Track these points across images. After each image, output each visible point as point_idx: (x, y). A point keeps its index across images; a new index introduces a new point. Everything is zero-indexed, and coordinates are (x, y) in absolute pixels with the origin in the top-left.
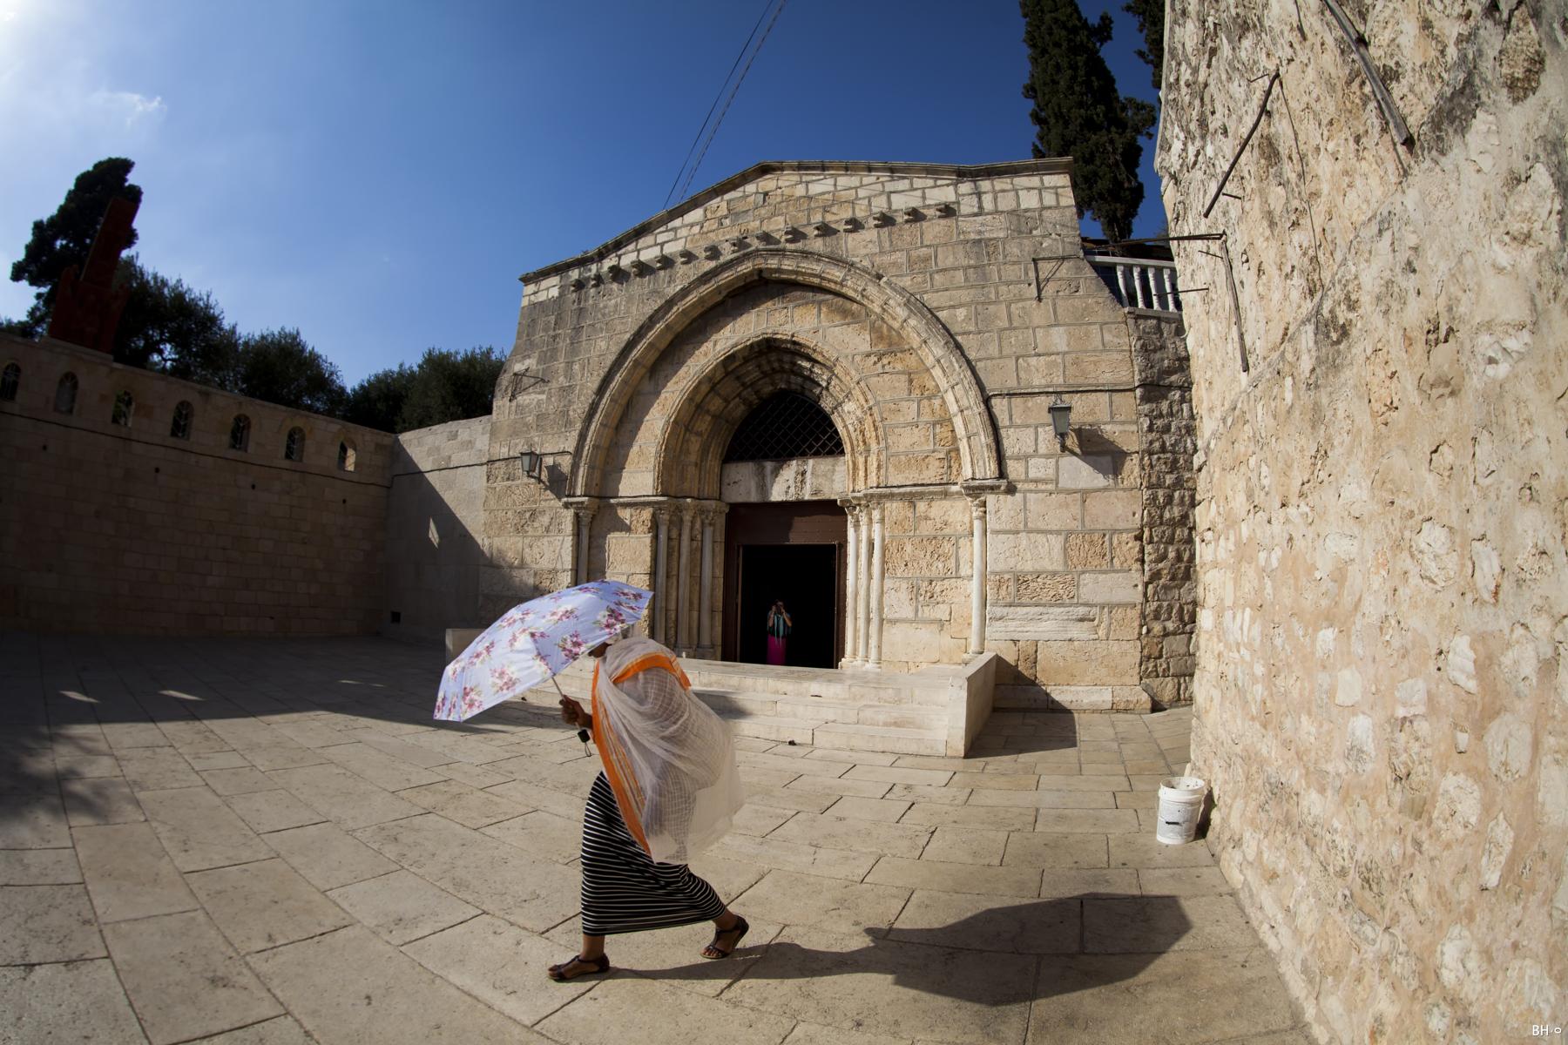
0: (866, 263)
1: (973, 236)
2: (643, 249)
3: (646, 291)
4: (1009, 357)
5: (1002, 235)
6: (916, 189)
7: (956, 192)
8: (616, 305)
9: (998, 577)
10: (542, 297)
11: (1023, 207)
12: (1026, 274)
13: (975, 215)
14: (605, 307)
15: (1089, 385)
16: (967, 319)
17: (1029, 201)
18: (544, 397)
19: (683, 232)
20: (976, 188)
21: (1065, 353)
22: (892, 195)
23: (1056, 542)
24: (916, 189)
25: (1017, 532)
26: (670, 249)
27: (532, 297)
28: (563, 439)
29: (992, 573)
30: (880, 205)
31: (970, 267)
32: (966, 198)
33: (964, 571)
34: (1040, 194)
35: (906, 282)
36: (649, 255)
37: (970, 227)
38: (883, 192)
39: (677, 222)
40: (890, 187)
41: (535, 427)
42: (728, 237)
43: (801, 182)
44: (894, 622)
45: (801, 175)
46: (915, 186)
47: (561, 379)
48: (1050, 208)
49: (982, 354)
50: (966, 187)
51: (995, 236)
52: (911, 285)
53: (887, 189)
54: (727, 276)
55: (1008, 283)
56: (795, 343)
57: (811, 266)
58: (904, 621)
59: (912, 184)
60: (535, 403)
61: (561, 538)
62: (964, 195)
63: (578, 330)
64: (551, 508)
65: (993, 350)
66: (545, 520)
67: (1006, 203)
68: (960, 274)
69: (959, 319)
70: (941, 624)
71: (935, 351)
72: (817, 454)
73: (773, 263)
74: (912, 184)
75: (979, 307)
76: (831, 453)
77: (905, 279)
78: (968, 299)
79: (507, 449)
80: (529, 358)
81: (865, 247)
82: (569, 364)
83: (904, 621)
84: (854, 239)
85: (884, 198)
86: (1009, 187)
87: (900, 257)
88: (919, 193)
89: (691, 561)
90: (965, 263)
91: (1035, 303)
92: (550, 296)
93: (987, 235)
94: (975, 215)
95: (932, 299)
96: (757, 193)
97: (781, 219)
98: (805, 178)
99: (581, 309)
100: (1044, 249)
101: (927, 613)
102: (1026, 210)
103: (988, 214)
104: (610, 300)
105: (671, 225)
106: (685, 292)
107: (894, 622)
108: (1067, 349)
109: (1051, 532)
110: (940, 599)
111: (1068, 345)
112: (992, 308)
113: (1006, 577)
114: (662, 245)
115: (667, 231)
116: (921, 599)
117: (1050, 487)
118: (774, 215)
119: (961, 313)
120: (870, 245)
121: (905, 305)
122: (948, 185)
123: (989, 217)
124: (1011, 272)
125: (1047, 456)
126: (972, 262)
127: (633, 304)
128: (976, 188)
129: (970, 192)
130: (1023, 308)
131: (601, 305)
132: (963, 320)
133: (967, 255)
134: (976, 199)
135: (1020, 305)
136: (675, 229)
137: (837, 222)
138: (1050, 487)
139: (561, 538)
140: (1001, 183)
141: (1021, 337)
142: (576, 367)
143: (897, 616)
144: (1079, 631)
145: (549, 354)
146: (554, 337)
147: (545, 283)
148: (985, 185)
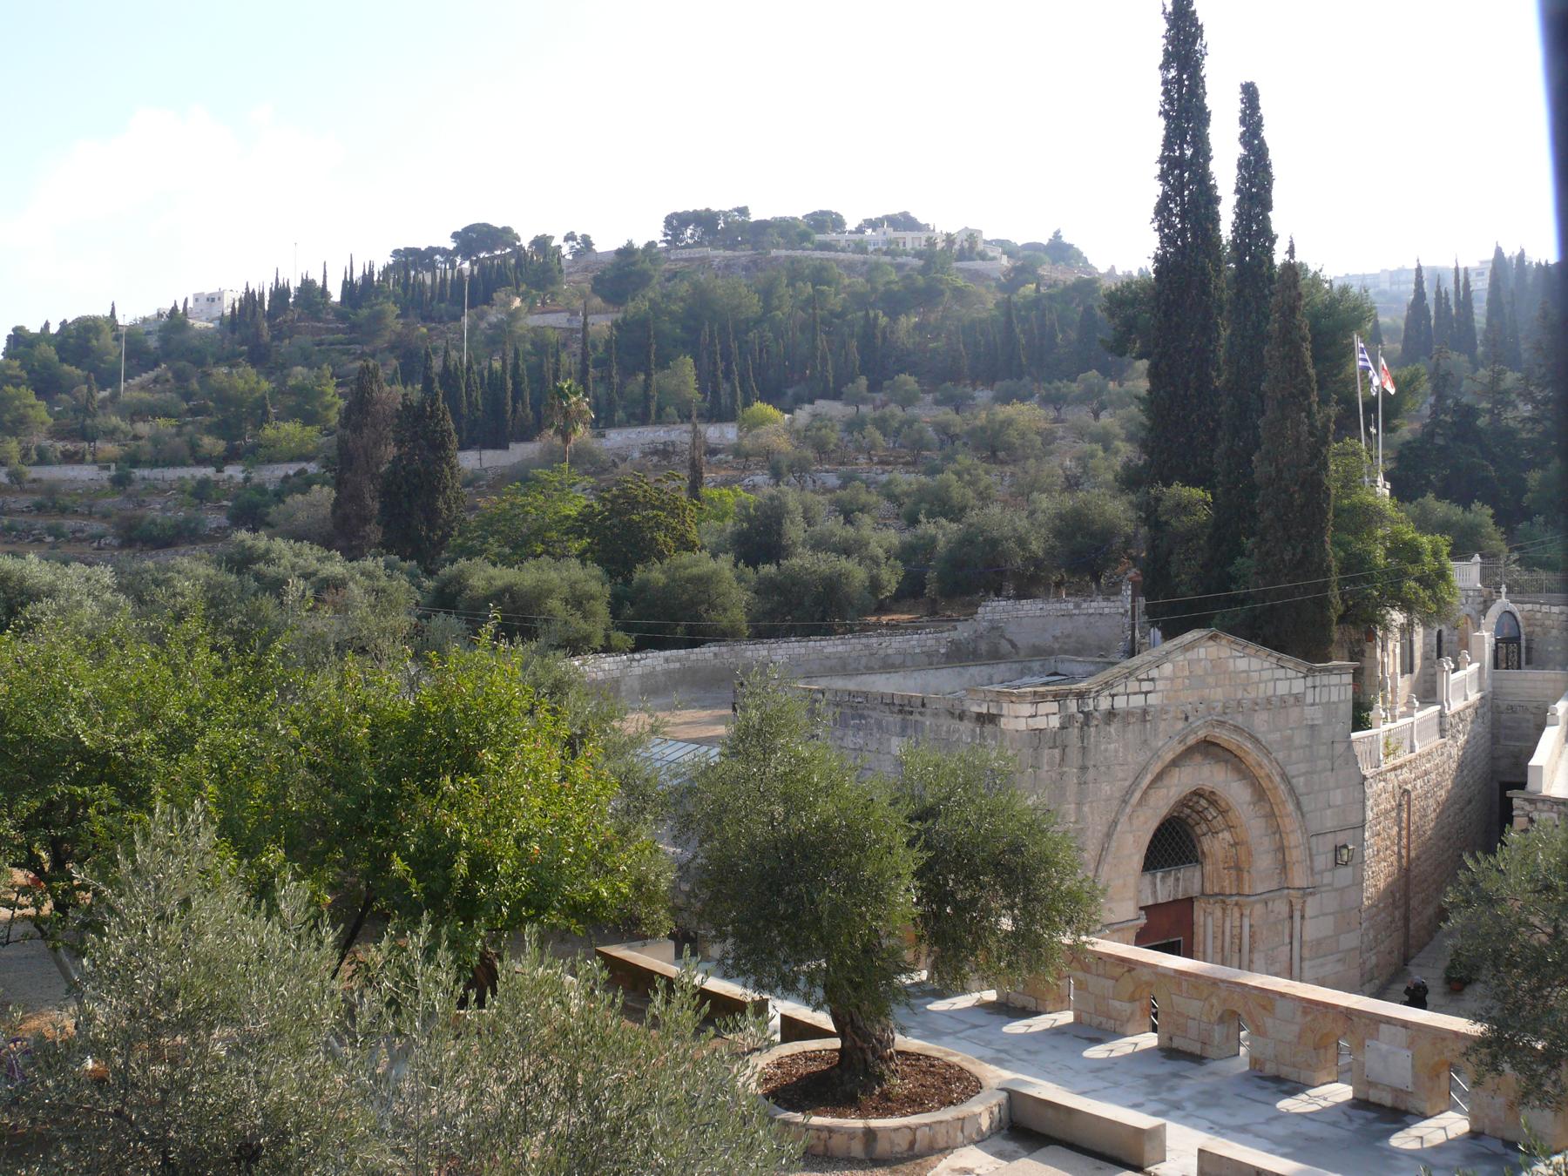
1: (1310, 723)
8: (1116, 751)
10: (1040, 723)
14: (1106, 750)
17: (1334, 698)
19: (1160, 685)
23: (1331, 918)
25: (1317, 917)
35: (1281, 756)
56: (1212, 792)
67: (1325, 700)
71: (1290, 807)
72: (1184, 863)
76: (1191, 862)
82: (1079, 804)
87: (1277, 736)
91: (1329, 773)
92: (1051, 725)
95: (1291, 770)
97: (1219, 690)
114: (1146, 693)
115: (1148, 680)
118: (1217, 686)
142: (1086, 809)
146: (1062, 774)
147: (1045, 707)
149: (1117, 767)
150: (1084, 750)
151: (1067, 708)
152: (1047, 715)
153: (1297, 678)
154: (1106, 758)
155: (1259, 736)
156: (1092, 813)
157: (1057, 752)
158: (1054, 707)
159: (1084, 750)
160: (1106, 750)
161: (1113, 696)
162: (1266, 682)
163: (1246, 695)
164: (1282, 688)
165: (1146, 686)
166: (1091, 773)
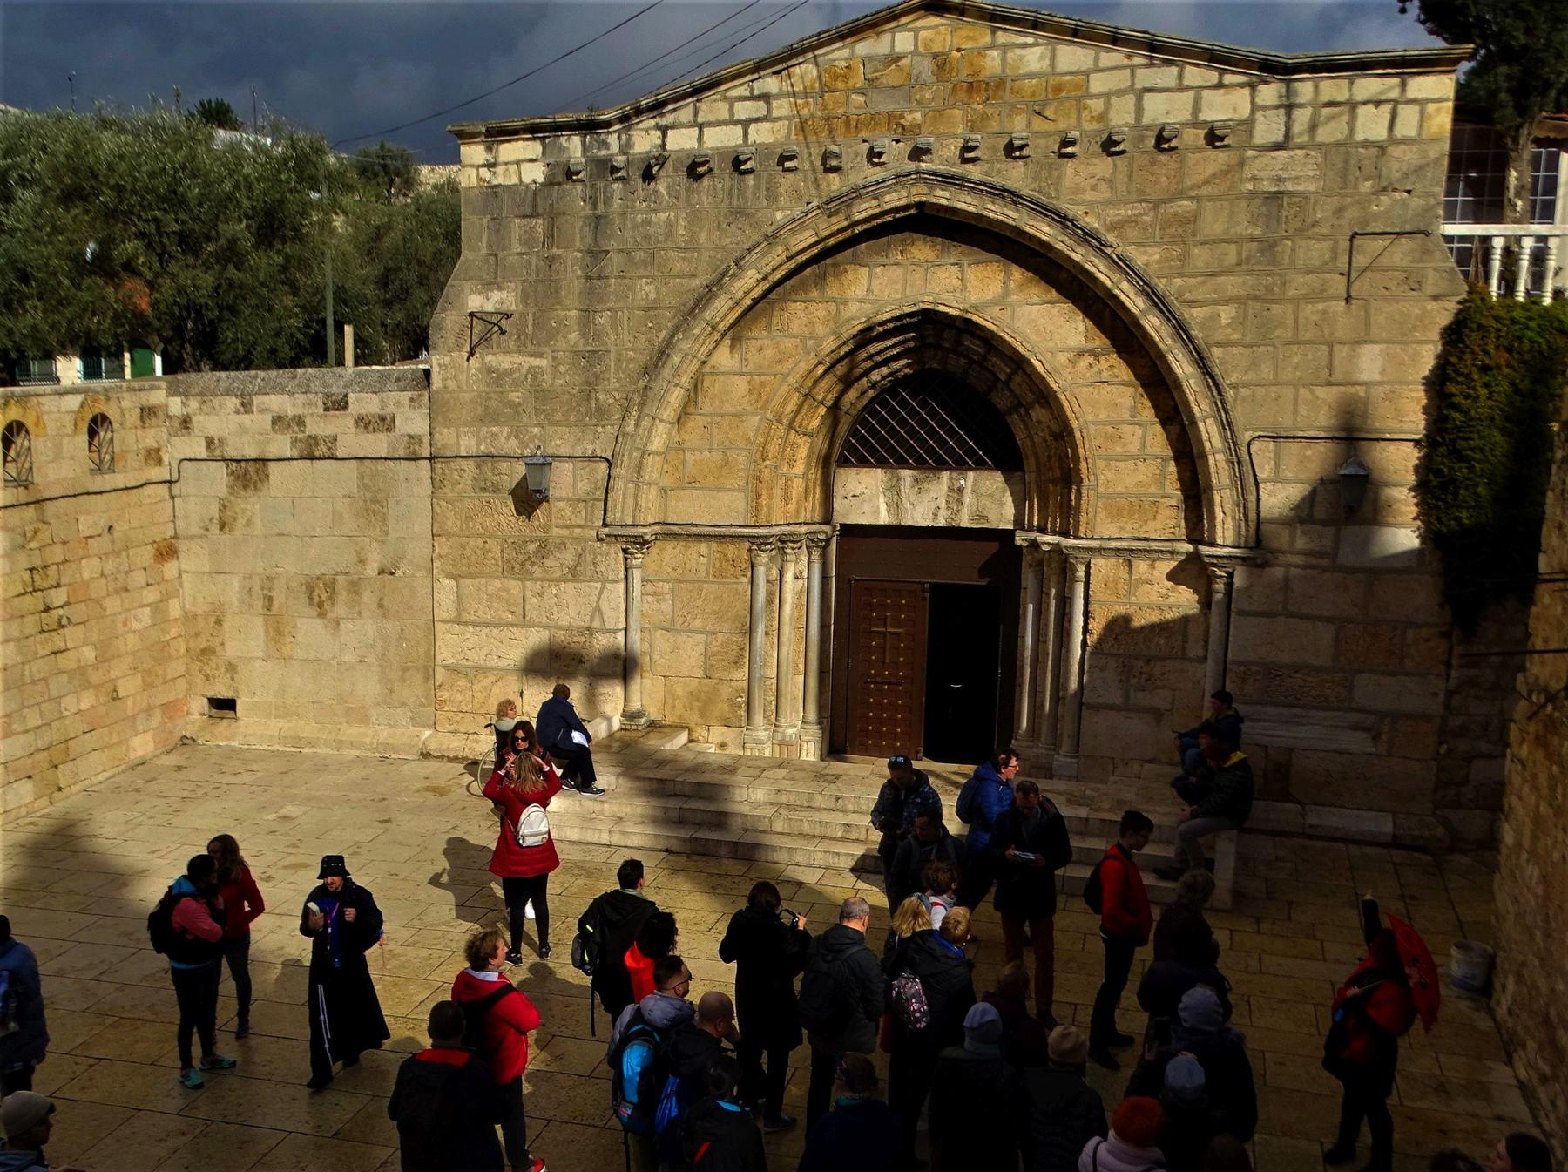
0: (1088, 219)
2: (710, 124)
3: (724, 206)
4: (1288, 383)
5: (1312, 188)
6: (1188, 88)
7: (1253, 102)
8: (670, 224)
9: (1242, 668)
11: (1359, 137)
12: (1335, 258)
13: (1278, 147)
15: (1402, 431)
16: (1232, 325)
18: (543, 363)
19: (781, 108)
20: (1289, 93)
21: (1380, 383)
22: (1148, 99)
24: (1188, 88)
26: (761, 134)
27: (485, 173)
28: (590, 437)
29: (1234, 662)
30: (1121, 116)
31: (1252, 239)
32: (1269, 113)
33: (1195, 650)
34: (1394, 115)
36: (721, 138)
37: (1265, 170)
38: (1131, 89)
39: (771, 84)
40: (1147, 77)
41: (530, 409)
42: (864, 134)
43: (992, 47)
44: (1098, 708)
45: (994, 31)
46: (1186, 82)
47: (573, 336)
48: (1404, 141)
49: (1251, 376)
50: (1270, 92)
51: (1300, 188)
52: (1158, 262)
53: (1139, 86)
54: (863, 209)
55: (1310, 271)
57: (1006, 211)
58: (1113, 707)
59: (1181, 76)
60: (524, 371)
61: (599, 585)
62: (1265, 108)
63: (596, 254)
64: (579, 539)
65: (1266, 372)
66: (569, 557)
68: (1233, 248)
69: (1224, 322)
70: (1158, 715)
73: (942, 197)
74: (1181, 76)
75: (1257, 305)
77: (1150, 250)
78: (1241, 292)
79: (474, 442)
80: (500, 289)
81: (1094, 188)
82: (587, 312)
83: (1113, 707)
84: (1076, 173)
85: (1130, 100)
86: (1343, 96)
88: (1191, 94)
89: (796, 607)
90: (1243, 228)
92: (527, 179)
93: (1289, 186)
94: (1278, 147)
96: (915, 53)
98: (1002, 37)
99: (598, 218)
100: (1376, 216)
101: (1140, 698)
102: (1366, 144)
103: (1301, 147)
104: (655, 211)
105: (759, 87)
106: (797, 224)
107: (1098, 708)
108: (1377, 377)
109: (1320, 618)
110: (1159, 683)
111: (1383, 372)
112: (1276, 309)
113: (1254, 668)
114: (746, 123)
115: (752, 98)
116: (1134, 681)
117: (1324, 562)
119: (1226, 314)
120: (1103, 186)
121: (1147, 295)
122: (1242, 85)
123: (1300, 152)
124: (1316, 251)
125: (1324, 523)
126: (1257, 232)
127: (702, 228)
128: (1288, 97)
129: (1276, 102)
130: (1325, 312)
131: (639, 218)
132: (1229, 325)
133: (1253, 222)
134: (1283, 118)
135: (1320, 306)
136: (766, 97)
137: (1047, 134)
138: (1324, 562)
139: (599, 585)
140: (1333, 87)
141: (1310, 357)
142: (603, 320)
143: (1101, 701)
144: (1357, 743)
145: (540, 287)
146: (551, 260)
147: (511, 150)
148: (1305, 89)
149: (672, 254)
150: (598, 222)
151: (562, 149)
152: (518, 163)
153: (1219, 85)
154: (647, 237)
155: (1074, 210)
156: (615, 327)
157: (539, 225)
158: (533, 148)
159: (598, 222)
160: (647, 223)
161: (664, 130)
162: (1107, 96)
163: (1038, 124)
164: (1165, 109)
165: (743, 110)
166: (615, 261)
